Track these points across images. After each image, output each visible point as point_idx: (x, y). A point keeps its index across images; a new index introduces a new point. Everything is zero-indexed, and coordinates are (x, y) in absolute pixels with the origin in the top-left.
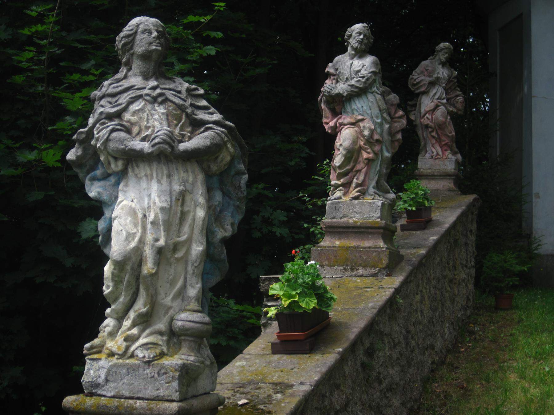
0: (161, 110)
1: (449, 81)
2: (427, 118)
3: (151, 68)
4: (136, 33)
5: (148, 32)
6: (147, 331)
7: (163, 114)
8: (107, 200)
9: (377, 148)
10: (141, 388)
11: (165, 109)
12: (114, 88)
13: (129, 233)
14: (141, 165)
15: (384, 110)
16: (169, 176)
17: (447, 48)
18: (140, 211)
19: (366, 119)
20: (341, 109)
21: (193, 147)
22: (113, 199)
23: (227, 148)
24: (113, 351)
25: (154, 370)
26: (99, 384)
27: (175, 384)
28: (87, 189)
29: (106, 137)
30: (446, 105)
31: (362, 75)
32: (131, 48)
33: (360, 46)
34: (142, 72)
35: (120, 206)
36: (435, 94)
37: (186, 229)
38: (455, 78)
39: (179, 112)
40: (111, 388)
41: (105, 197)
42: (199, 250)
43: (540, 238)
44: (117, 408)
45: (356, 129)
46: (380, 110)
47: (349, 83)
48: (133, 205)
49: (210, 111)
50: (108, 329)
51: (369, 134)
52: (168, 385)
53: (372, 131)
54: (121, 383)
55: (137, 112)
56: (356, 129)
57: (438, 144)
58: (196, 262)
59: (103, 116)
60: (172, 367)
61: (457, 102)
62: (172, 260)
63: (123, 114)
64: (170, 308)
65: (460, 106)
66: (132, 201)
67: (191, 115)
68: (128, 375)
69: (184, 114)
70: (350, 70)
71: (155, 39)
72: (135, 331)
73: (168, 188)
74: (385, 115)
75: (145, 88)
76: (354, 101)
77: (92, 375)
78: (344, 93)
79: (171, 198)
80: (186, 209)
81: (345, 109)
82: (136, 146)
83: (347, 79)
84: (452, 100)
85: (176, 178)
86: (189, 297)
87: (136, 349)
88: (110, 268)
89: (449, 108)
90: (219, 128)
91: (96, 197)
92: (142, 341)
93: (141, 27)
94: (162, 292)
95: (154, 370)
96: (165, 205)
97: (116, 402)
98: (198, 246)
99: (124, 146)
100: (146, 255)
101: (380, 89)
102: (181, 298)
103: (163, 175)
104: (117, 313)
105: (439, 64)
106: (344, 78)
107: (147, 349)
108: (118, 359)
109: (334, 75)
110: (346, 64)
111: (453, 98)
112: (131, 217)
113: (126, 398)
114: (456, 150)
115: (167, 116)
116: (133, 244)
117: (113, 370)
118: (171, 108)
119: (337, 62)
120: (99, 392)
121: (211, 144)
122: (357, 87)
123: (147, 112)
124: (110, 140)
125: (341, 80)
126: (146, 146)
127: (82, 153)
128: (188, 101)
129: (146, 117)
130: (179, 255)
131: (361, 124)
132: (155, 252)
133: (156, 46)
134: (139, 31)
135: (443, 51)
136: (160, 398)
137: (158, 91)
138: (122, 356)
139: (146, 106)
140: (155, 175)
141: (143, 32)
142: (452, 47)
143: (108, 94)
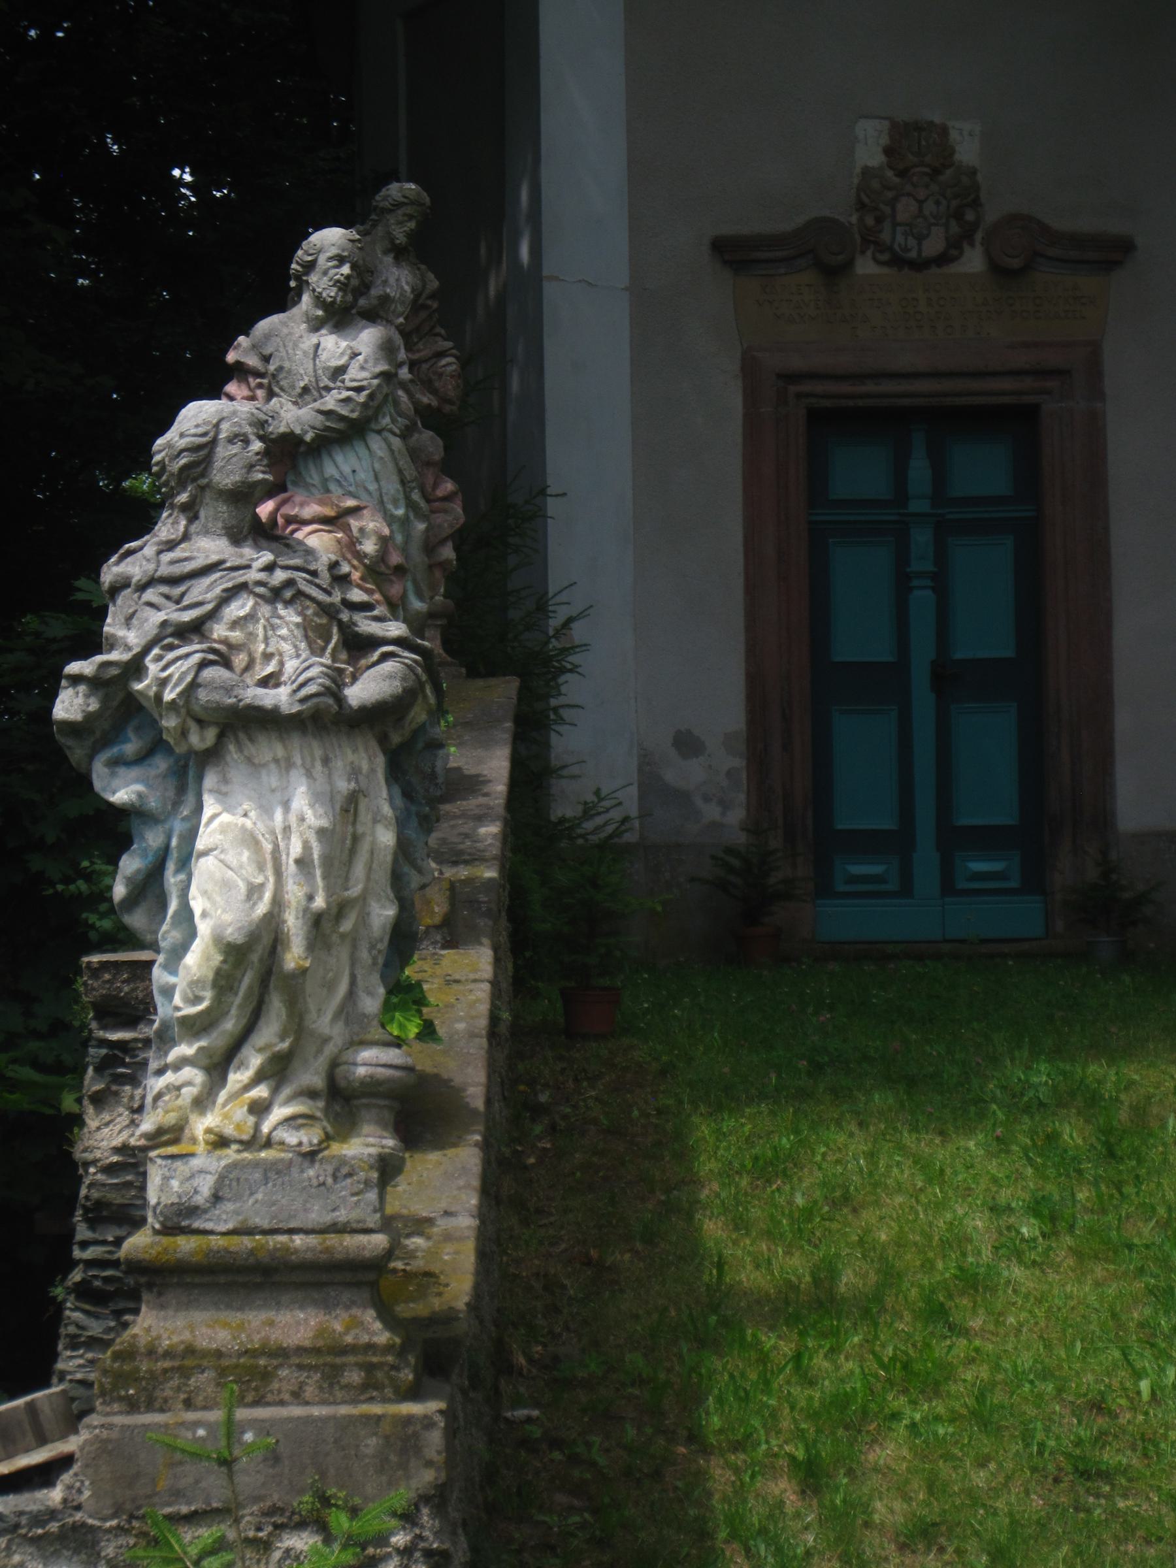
0: (291, 616)
1: (416, 306)
3: (247, 519)
4: (214, 442)
5: (241, 441)
6: (287, 1091)
7: (297, 625)
8: (157, 809)
9: (395, 590)
10: (296, 1210)
11: (300, 614)
12: (173, 562)
13: (252, 884)
14: (262, 739)
15: (412, 481)
16: (326, 761)
17: (412, 203)
18: (267, 836)
19: (365, 507)
20: (286, 474)
21: (373, 700)
22: (170, 807)
23: (425, 697)
24: (225, 1135)
25: (325, 1170)
26: (197, 1208)
27: (372, 1196)
28: (98, 785)
29: (189, 679)
30: (411, 387)
31: (355, 384)
32: (203, 475)
33: (342, 297)
34: (229, 528)
35: (216, 824)
37: (359, 870)
38: (432, 296)
39: (324, 621)
40: (227, 1213)
41: (153, 803)
42: (388, 916)
43: (619, 794)
44: (252, 1252)
45: (339, 535)
46: (403, 482)
47: (317, 405)
48: (248, 823)
49: (376, 613)
50: (189, 1093)
51: (377, 551)
52: (355, 1198)
53: (384, 541)
54: (251, 1201)
55: (242, 622)
56: (339, 535)
58: (381, 940)
59: (170, 630)
60: (364, 1162)
62: (335, 938)
63: (208, 625)
64: (326, 1040)
65: (450, 388)
66: (245, 815)
67: (349, 627)
68: (266, 1184)
69: (335, 623)
70: (315, 365)
71: (259, 457)
72: (261, 1091)
73: (328, 788)
74: (416, 496)
75: (248, 567)
76: (331, 456)
77: (176, 1189)
78: (306, 432)
79: (333, 807)
80: (360, 829)
81: (299, 474)
82: (261, 700)
83: (306, 390)
84: (425, 366)
85: (340, 764)
86: (364, 1015)
87: (275, 1128)
88: (207, 958)
89: (418, 396)
90: (406, 654)
91: (133, 805)
92: (279, 1113)
93: (224, 426)
94: (312, 1007)
95: (325, 1170)
96: (324, 823)
97: (247, 1242)
98: (383, 907)
99: (235, 700)
100: (288, 930)
101: (399, 419)
102: (343, 1017)
103: (313, 760)
104: (211, 1057)
105: (386, 252)
106: (293, 387)
107: (298, 1128)
108: (239, 1151)
109: (258, 374)
110: (301, 346)
111: (426, 361)
112: (249, 849)
113: (265, 1232)
115: (305, 630)
116: (262, 908)
117: (231, 1176)
118: (309, 612)
119: (268, 337)
120: (197, 1224)
121: (405, 690)
122: (342, 418)
123: (262, 621)
124: (199, 686)
125: (282, 389)
126: (281, 698)
127: (100, 707)
128: (335, 594)
129: (260, 632)
130: (347, 926)
131: (355, 524)
132: (309, 924)
133: (264, 472)
134: (222, 436)
135: (400, 212)
136: (339, 1226)
137: (280, 576)
138: (247, 1145)
139: (257, 607)
140: (298, 761)
141: (231, 440)
142: (427, 200)
143: (161, 577)
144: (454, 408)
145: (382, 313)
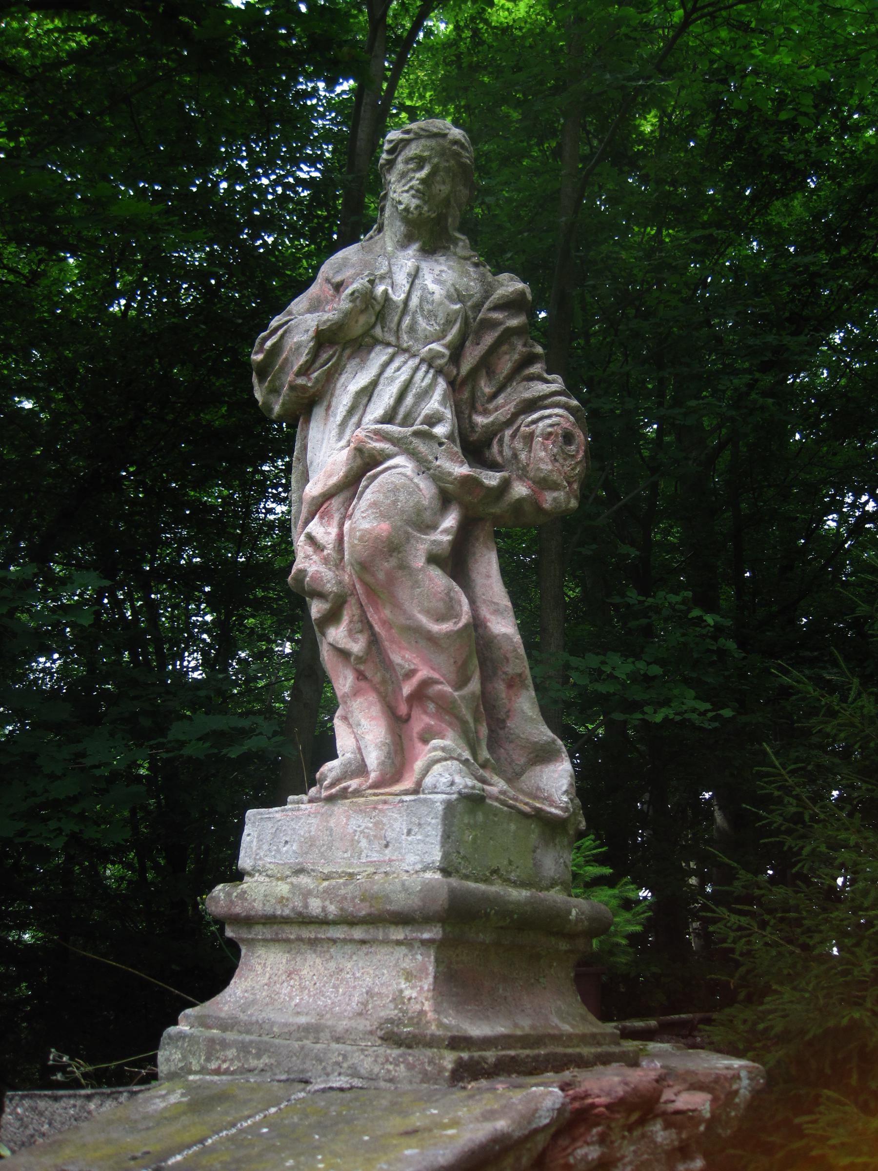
2: (311, 538)
36: (368, 392)
57: (372, 697)
61: (529, 438)
84: (508, 433)
111: (509, 423)
114: (544, 733)
135: (400, 159)
144: (560, 495)
145: (378, 331)
